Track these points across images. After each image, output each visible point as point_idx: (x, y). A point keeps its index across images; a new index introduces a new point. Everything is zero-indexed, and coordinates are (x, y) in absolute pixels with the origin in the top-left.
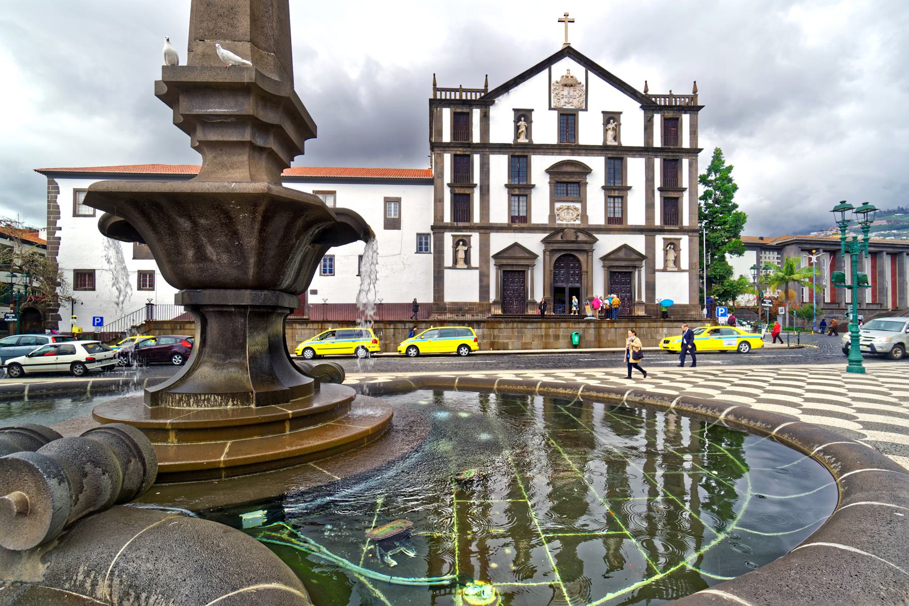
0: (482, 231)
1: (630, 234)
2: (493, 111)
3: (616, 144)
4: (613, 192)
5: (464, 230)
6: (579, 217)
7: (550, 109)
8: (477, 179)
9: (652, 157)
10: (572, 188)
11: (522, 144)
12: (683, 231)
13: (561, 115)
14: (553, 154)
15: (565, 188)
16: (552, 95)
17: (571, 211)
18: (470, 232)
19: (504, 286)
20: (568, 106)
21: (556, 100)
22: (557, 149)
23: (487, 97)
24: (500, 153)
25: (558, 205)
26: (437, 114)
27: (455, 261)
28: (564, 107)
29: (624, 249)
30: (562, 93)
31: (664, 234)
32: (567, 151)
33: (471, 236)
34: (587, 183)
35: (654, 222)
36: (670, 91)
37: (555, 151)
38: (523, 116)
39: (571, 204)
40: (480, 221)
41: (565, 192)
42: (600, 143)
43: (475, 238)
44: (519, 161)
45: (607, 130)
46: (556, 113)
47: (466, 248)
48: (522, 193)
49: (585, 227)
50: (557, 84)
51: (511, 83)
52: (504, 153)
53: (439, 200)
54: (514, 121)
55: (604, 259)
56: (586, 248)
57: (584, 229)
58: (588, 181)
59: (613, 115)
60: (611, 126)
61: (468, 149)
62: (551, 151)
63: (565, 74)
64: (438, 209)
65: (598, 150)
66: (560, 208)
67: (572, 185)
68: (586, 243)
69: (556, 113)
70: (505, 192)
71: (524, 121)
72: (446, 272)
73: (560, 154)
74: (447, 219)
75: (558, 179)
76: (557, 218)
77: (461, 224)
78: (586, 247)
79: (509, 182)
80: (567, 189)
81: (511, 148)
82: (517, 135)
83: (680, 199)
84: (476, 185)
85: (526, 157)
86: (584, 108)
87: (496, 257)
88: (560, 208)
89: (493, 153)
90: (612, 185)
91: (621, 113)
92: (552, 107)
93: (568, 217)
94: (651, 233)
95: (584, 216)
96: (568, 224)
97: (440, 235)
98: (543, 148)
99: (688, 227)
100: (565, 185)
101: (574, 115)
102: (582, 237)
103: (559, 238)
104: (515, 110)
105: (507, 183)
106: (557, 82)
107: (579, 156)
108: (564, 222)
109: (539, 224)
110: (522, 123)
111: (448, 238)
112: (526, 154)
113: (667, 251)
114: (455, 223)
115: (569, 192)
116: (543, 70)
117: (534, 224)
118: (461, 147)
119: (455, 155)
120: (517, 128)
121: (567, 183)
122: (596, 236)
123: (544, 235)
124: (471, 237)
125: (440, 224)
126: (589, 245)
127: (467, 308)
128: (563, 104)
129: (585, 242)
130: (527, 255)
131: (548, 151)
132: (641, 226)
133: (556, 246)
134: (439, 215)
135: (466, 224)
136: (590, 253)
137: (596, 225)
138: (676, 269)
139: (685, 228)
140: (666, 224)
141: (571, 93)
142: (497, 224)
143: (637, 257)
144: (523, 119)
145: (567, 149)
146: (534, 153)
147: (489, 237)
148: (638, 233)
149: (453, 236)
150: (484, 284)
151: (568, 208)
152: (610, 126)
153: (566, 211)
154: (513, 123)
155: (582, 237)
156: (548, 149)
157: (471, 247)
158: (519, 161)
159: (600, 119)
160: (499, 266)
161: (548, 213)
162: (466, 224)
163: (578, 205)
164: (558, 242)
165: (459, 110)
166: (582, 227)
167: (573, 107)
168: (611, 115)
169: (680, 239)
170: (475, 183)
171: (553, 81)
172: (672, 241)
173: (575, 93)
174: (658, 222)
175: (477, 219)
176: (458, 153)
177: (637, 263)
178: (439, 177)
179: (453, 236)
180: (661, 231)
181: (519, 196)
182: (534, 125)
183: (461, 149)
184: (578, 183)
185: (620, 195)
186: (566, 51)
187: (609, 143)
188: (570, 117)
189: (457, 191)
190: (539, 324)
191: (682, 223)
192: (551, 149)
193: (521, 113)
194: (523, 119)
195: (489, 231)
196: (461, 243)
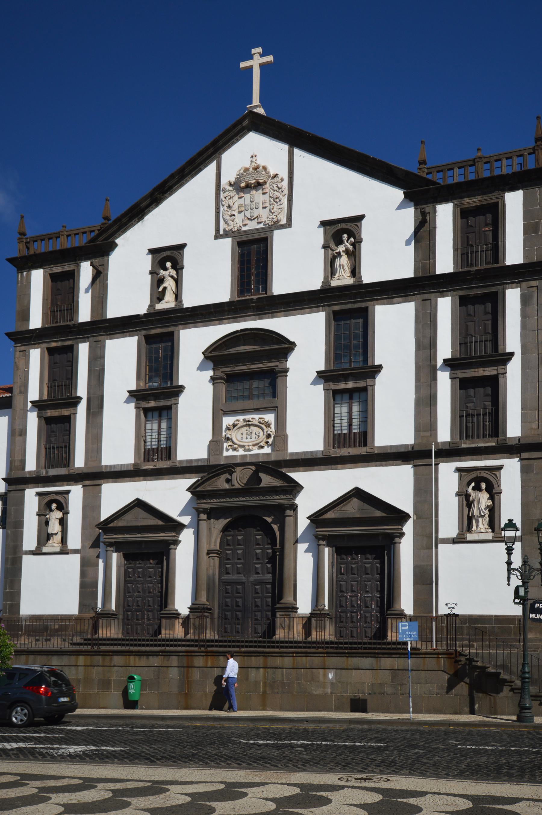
6: (270, 441)
9: (432, 296)
16: (222, 209)
17: (254, 429)
18: (67, 485)
19: (126, 582)
20: (253, 225)
21: (227, 217)
23: (101, 238)
26: (22, 283)
28: (244, 229)
30: (241, 201)
31: (460, 461)
33: (68, 492)
38: (168, 259)
46: (227, 243)
49: (280, 458)
50: (231, 188)
59: (344, 226)
63: (247, 164)
66: (234, 426)
69: (229, 240)
72: (25, 558)
78: (278, 500)
79: (138, 385)
83: (501, 380)
84: (80, 398)
86: (284, 221)
90: (347, 366)
91: (360, 218)
92: (222, 232)
93: (247, 441)
96: (245, 456)
97: (18, 494)
99: (519, 439)
103: (221, 483)
104: (153, 252)
105: (134, 388)
108: (241, 452)
110: (169, 272)
113: (467, 496)
117: (181, 461)
120: (158, 282)
122: (294, 475)
127: (57, 627)
130: (160, 523)
132: (407, 446)
133: (214, 503)
135: (62, 471)
139: (509, 443)
140: (467, 437)
142: (115, 466)
150: (88, 580)
153: (244, 430)
155: (267, 480)
161: (210, 438)
165: (57, 269)
166: (273, 458)
167: (261, 226)
168: (340, 226)
170: (79, 394)
171: (224, 181)
172: (483, 474)
176: (54, 345)
177: (389, 528)
178: (21, 392)
182: (186, 273)
187: (334, 283)
189: (49, 413)
190: (73, 658)
193: (164, 254)
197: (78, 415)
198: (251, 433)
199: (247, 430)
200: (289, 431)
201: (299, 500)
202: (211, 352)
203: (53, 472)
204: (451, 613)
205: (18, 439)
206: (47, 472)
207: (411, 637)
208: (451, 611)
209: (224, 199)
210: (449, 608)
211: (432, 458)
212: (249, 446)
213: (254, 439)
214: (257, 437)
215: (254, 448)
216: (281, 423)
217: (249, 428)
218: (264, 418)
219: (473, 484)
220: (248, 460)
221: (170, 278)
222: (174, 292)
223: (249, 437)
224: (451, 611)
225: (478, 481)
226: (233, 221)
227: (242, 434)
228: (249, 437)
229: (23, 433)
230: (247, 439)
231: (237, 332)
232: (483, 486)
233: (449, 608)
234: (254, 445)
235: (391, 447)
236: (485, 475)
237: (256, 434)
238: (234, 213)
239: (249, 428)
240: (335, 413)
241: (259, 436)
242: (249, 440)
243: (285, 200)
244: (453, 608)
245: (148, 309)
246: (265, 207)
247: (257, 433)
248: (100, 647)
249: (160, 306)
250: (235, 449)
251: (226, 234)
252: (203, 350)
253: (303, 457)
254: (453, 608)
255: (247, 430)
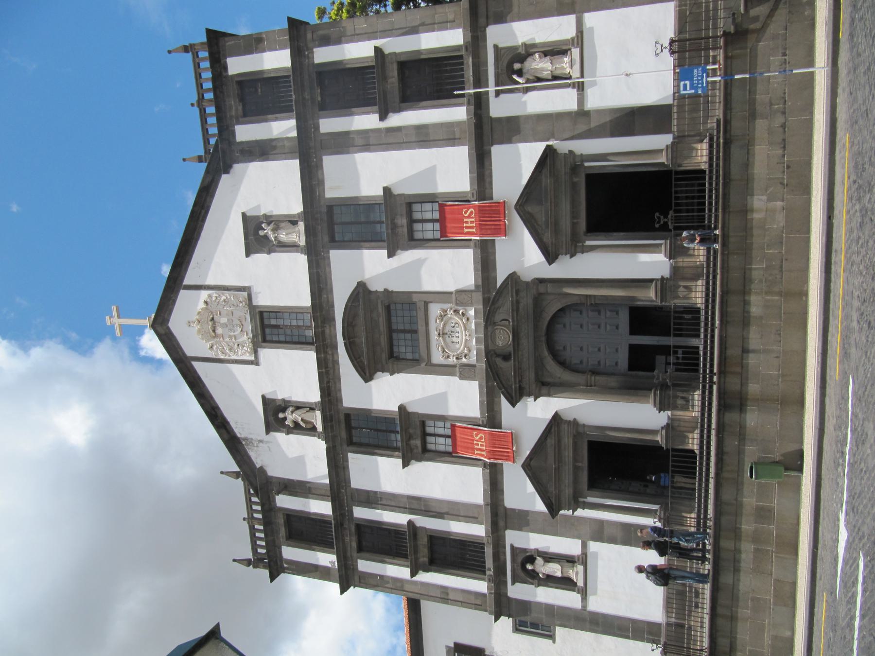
0: (501, 524)
1: (491, 183)
2: (275, 471)
3: (301, 225)
4: (400, 230)
5: (502, 557)
7: (256, 362)
8: (400, 519)
10: (400, 320)
11: (324, 427)
12: (476, 40)
13: (265, 340)
14: (336, 363)
15: (402, 336)
18: (505, 547)
20: (249, 327)
22: (326, 353)
24: (345, 468)
25: (437, 357)
27: (566, 583)
28: (251, 335)
29: (529, 208)
32: (327, 331)
34: (386, 290)
35: (459, 124)
36: (192, 105)
37: (329, 357)
39: (435, 326)
40: (481, 523)
41: (408, 336)
42: (301, 261)
43: (514, 538)
44: (356, 428)
45: (279, 242)
47: (539, 561)
48: (419, 432)
49: (481, 298)
50: (215, 347)
51: (226, 436)
52: (346, 460)
53: (444, 596)
54: (288, 434)
55: (551, 256)
56: (530, 301)
57: (486, 301)
58: (381, 289)
60: (268, 231)
61: (346, 526)
62: (330, 365)
64: (461, 599)
65: (318, 266)
66: (444, 351)
67: (394, 319)
68: (518, 302)
70: (417, 467)
71: (284, 410)
73: (335, 347)
74: (481, 586)
75: (384, 356)
76: (464, 360)
77: (489, 563)
78: (527, 301)
79: (398, 457)
80: (404, 331)
81: (334, 447)
82: (311, 430)
84: (410, 523)
85: (348, 416)
86: (245, 294)
87: (553, 508)
88: (444, 351)
89: (347, 481)
92: (253, 358)
94: (486, 128)
95: (460, 297)
98: (328, 382)
100: (395, 336)
101: (261, 313)
102: (505, 311)
103: (507, 367)
106: (211, 347)
107: (333, 306)
109: (481, 402)
110: (291, 417)
111: (517, 591)
112: (342, 417)
114: (488, 573)
115: (408, 327)
116: (195, 372)
118: (343, 541)
119: (360, 549)
120: (296, 428)
121: (391, 331)
123: (504, 402)
124: (516, 545)
125: (490, 602)
126: (523, 294)
128: (245, 337)
129: (516, 304)
131: (331, 372)
134: (472, 599)
135: (489, 552)
136: (542, 289)
137: (476, 269)
138: (576, 52)
141: (224, 320)
142: (484, 490)
143: (546, 171)
144: (281, 415)
145: (323, 333)
146: (339, 400)
147: (513, 510)
148: (486, 163)
149: (513, 584)
151: (442, 334)
152: (272, 237)
153: (448, 340)
154: (291, 436)
156: (327, 373)
157: (537, 550)
158: (356, 428)
159: (260, 258)
160: (576, 503)
161: (455, 379)
162: (489, 552)
163: (435, 310)
164: (519, 372)
167: (248, 316)
169: (496, 47)
173: (224, 312)
174: (459, 113)
175: (478, 530)
179: (513, 584)
180: (479, 104)
181: (425, 435)
183: (347, 539)
184: (388, 308)
185: (404, 210)
186: (159, 329)
188: (266, 322)
189: (424, 559)
191: (457, 48)
192: (326, 367)
194: (281, 415)
195: (501, 512)
196: (529, 567)
197: (428, 527)
198: (452, 332)
199: (449, 337)
200: (452, 289)
201: (527, 276)
202: (365, 373)
203: (489, 563)
204: (669, 48)
205: (451, 596)
206: (490, 570)
207: (703, 77)
208: (666, 48)
209: (224, 355)
210: (662, 51)
211: (474, 88)
212: (466, 335)
213: (460, 329)
214: (457, 325)
215: (468, 328)
216: (442, 296)
217: (447, 334)
218: (435, 317)
219: (515, 77)
220: (482, 335)
221: (294, 414)
222: (307, 412)
223: (457, 335)
224: (666, 48)
225: (511, 71)
226: (244, 347)
227: (453, 342)
228: (457, 335)
229: (445, 590)
230: (458, 337)
231: (345, 344)
232: (517, 66)
233: (662, 51)
234: (465, 329)
235: (470, 173)
236: (505, 64)
237: (454, 327)
238: (236, 345)
239: (447, 334)
240: (433, 238)
241: (456, 323)
242: (459, 335)
243: (227, 293)
244: (662, 46)
245: (322, 440)
246: (232, 313)
247: (453, 325)
248: (709, 517)
249: (320, 427)
250: (470, 351)
251: (256, 352)
252: (363, 382)
253: (480, 273)
254: (662, 46)
255: (449, 337)
